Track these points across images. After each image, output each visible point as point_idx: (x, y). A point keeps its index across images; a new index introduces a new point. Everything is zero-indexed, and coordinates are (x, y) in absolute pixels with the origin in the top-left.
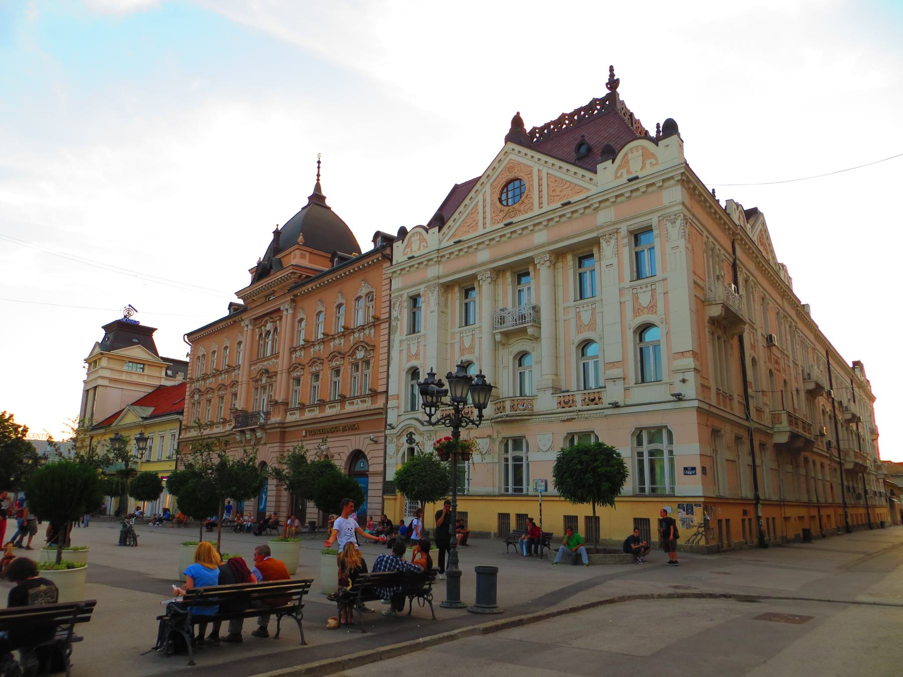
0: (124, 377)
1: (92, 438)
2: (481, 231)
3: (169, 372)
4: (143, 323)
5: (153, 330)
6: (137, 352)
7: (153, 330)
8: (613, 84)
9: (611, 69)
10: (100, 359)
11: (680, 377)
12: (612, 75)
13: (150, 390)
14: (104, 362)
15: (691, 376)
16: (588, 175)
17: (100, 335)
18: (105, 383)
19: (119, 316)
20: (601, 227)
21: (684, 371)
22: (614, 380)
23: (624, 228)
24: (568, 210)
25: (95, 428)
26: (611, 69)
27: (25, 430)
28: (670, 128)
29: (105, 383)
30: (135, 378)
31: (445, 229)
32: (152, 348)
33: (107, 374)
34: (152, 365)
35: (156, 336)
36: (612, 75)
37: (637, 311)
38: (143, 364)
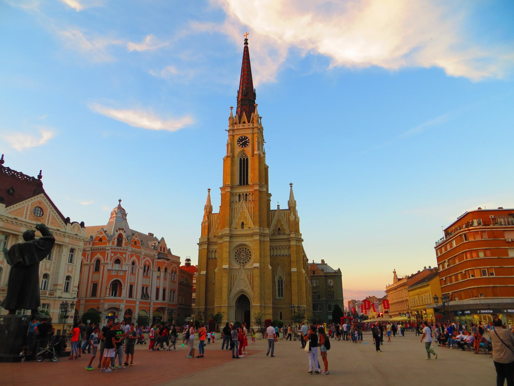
2: (23, 219)
8: (40, 177)
9: (41, 171)
11: (74, 292)
12: (40, 174)
15: (76, 293)
16: (64, 224)
20: (64, 242)
21: (75, 291)
22: (59, 289)
23: (70, 246)
24: (58, 232)
26: (41, 171)
28: (82, 224)
31: (8, 208)
36: (40, 174)
37: (68, 271)
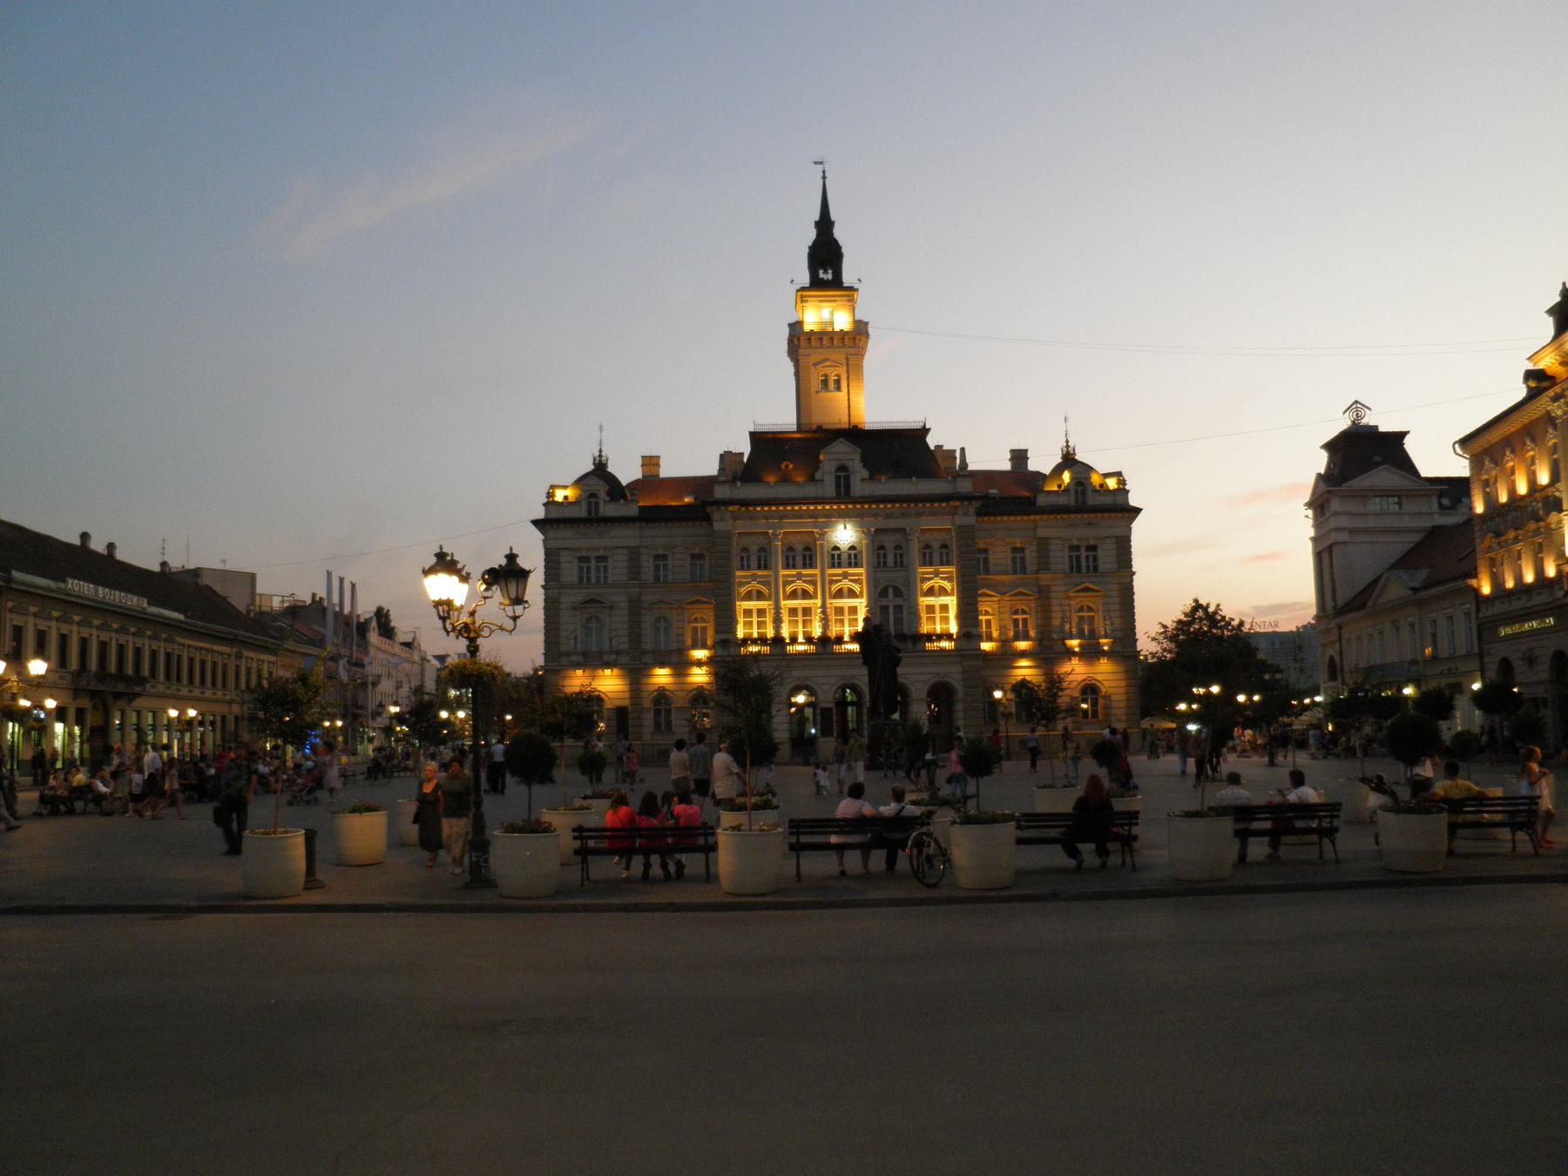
0: (1371, 523)
1: (1340, 628)
3: (1445, 501)
4: (1384, 428)
5: (1403, 435)
6: (1383, 477)
7: (1403, 435)
10: (1328, 500)
13: (1417, 538)
14: (1335, 505)
17: (1320, 462)
18: (1344, 537)
19: (1344, 424)
25: (1340, 611)
27: (1242, 623)
29: (1344, 537)
30: (1388, 522)
32: (1405, 464)
33: (1344, 522)
34: (1412, 494)
35: (1410, 445)
38: (1400, 495)
